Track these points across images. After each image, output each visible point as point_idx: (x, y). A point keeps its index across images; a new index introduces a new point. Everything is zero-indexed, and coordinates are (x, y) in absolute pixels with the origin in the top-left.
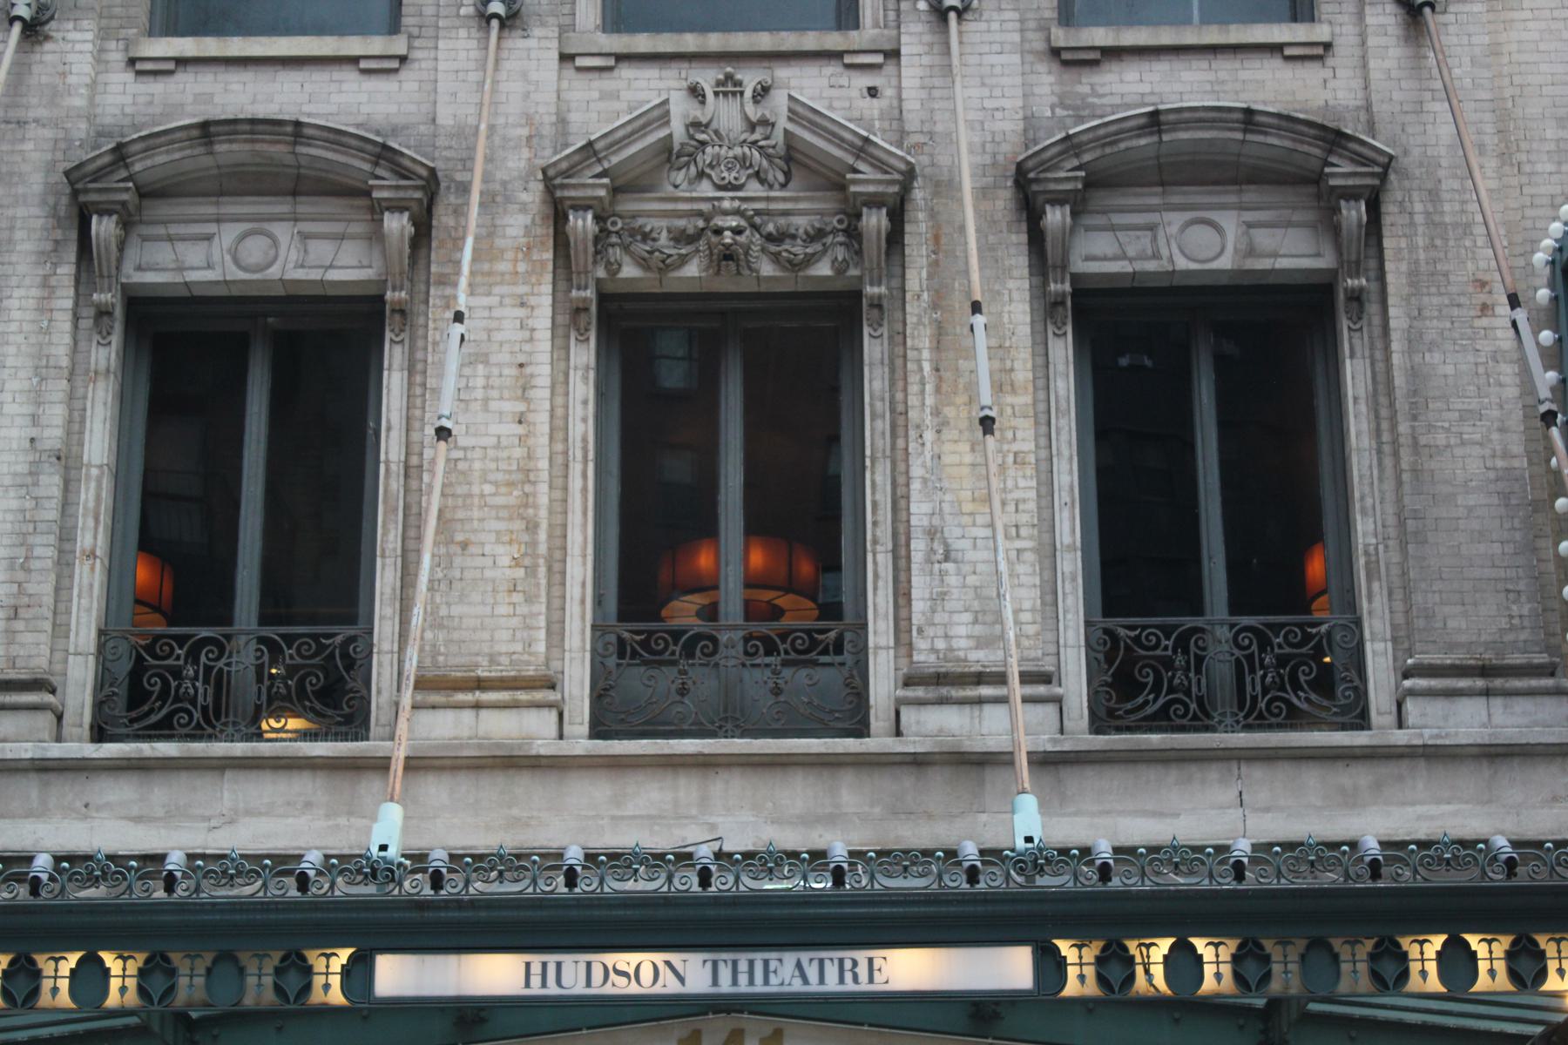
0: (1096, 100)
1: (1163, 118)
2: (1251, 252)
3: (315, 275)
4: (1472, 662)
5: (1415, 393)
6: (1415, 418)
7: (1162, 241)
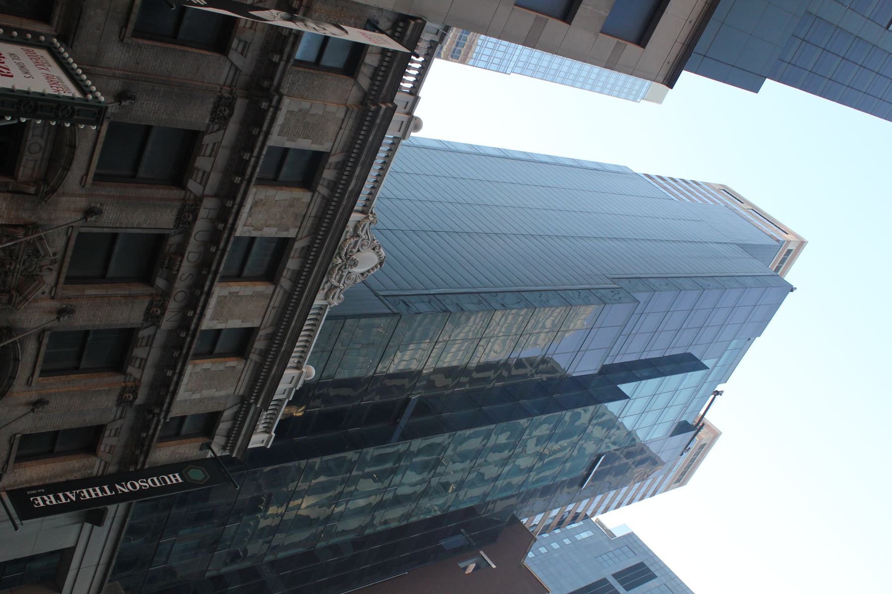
3: (23, 163)
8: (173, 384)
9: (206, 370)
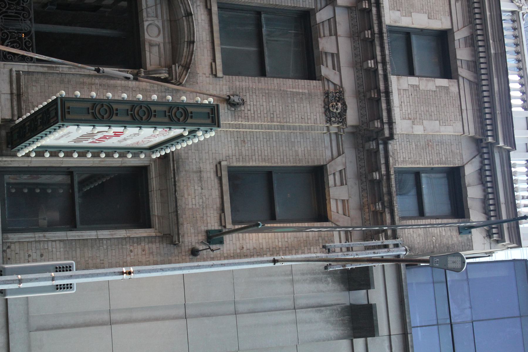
0: (195, 6)
1: (190, 17)
2: (151, 45)
4: (22, 91)
5: (108, 86)
6: (100, 85)
7: (153, 19)
8: (381, 78)
9: (415, 87)
